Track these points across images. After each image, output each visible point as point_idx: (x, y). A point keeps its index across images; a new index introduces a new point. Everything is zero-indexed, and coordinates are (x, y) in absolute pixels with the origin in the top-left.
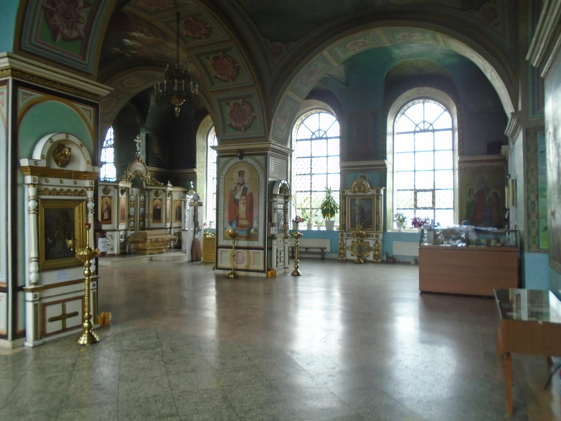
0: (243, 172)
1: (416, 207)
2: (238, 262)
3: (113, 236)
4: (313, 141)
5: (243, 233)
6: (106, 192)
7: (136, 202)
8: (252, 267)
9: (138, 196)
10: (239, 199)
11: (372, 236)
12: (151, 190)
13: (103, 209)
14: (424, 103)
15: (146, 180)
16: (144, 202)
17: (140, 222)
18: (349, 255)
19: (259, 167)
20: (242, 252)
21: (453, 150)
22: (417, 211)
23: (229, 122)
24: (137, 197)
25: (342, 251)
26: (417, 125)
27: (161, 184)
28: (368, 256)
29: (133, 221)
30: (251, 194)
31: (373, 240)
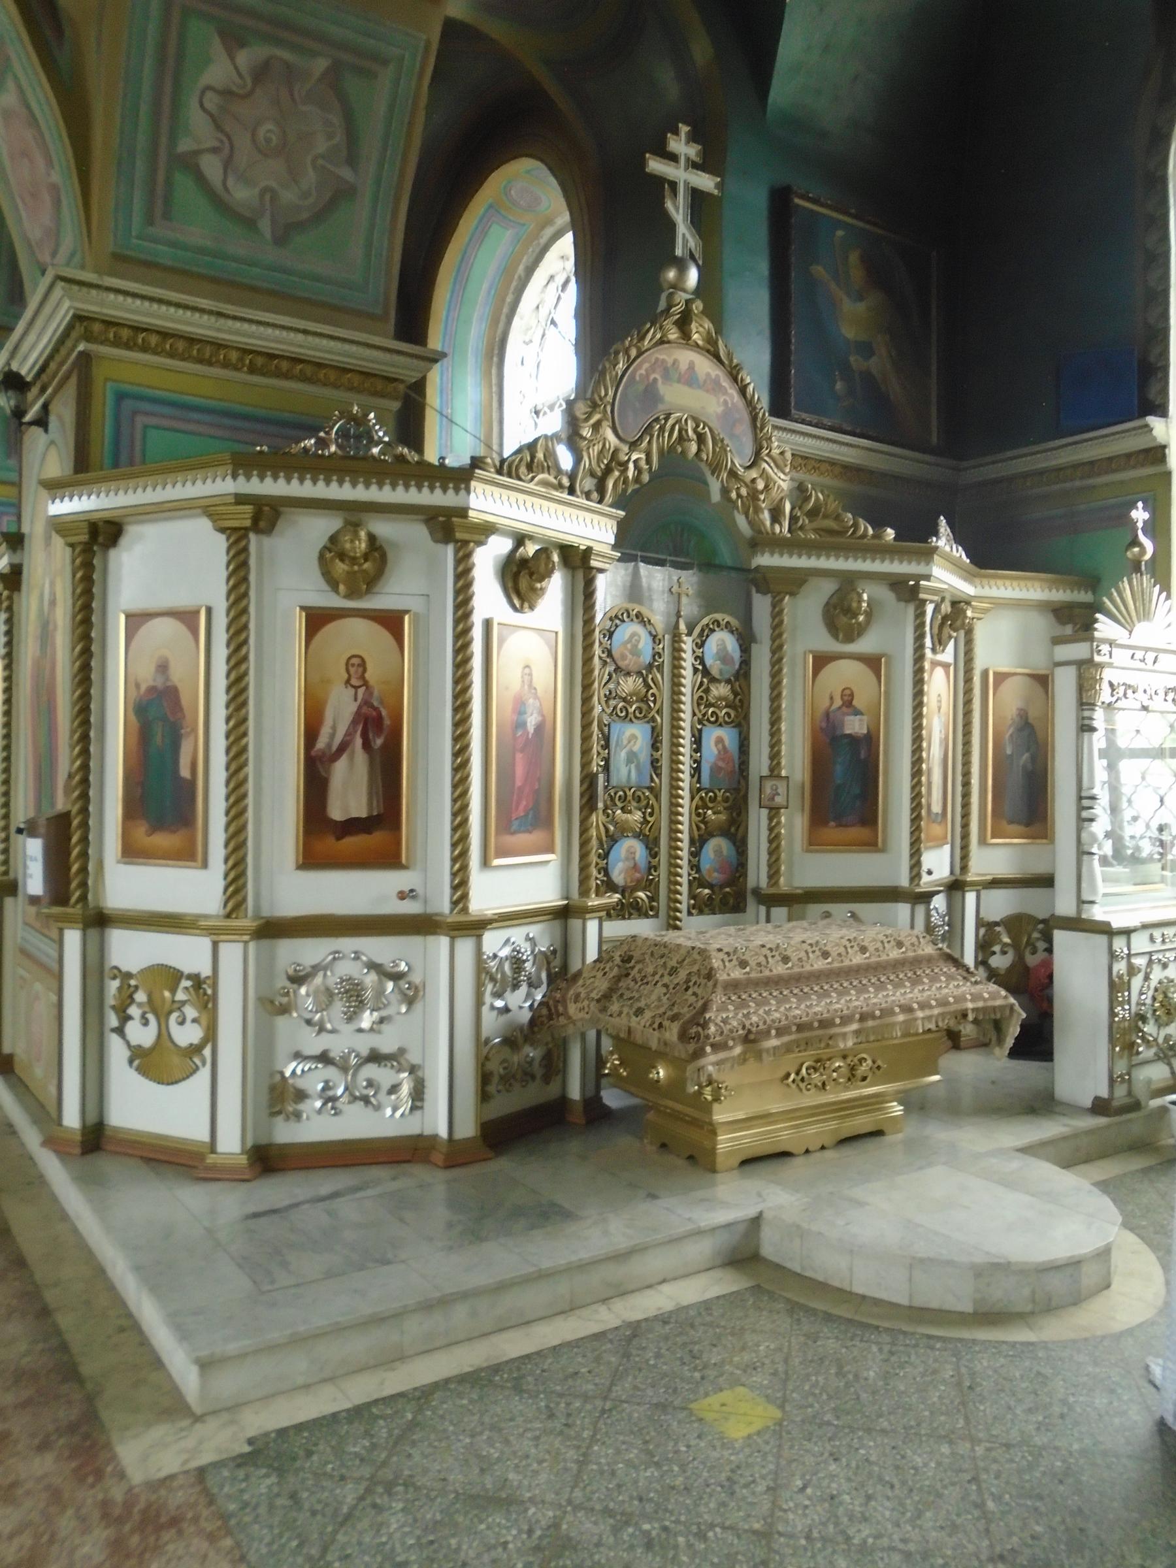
6: (341, 567)
7: (664, 680)
9: (683, 627)
12: (795, 581)
13: (325, 731)
15: (754, 495)
16: (742, 675)
17: (698, 844)
24: (676, 638)
29: (638, 835)
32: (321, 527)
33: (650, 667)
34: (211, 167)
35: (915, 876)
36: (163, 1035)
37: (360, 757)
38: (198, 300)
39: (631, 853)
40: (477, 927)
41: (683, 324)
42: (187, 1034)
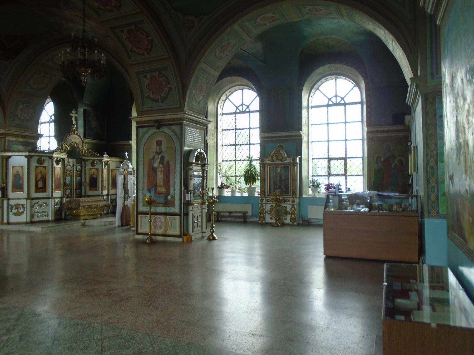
0: (161, 141)
1: (329, 174)
2: (157, 227)
3: (47, 203)
4: (237, 115)
5: (162, 200)
6: (40, 162)
7: (72, 172)
8: (169, 232)
9: (74, 166)
10: (157, 167)
11: (289, 201)
12: (87, 160)
14: (336, 80)
15: (82, 151)
16: (81, 171)
17: (76, 190)
18: (268, 219)
19: (175, 137)
20: (160, 218)
21: (362, 121)
22: (330, 177)
23: (147, 94)
24: (73, 166)
25: (262, 215)
26: (330, 100)
27: (97, 155)
28: (286, 219)
30: (168, 163)
31: (290, 204)
32: (37, 158)
33: (70, 170)
34: (19, 116)
35: (102, 193)
36: (18, 211)
37: (41, 181)
38: (30, 140)
39: (68, 191)
40: (54, 198)
41: (74, 132)
42: (21, 210)
